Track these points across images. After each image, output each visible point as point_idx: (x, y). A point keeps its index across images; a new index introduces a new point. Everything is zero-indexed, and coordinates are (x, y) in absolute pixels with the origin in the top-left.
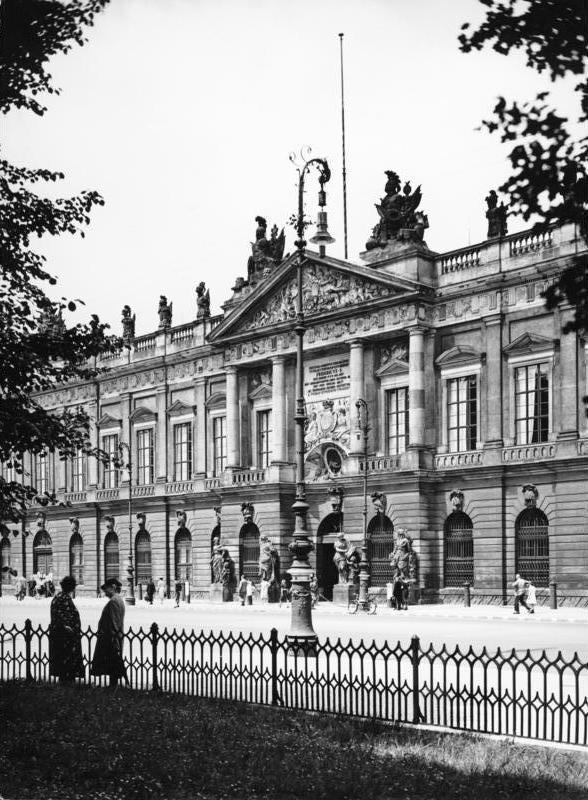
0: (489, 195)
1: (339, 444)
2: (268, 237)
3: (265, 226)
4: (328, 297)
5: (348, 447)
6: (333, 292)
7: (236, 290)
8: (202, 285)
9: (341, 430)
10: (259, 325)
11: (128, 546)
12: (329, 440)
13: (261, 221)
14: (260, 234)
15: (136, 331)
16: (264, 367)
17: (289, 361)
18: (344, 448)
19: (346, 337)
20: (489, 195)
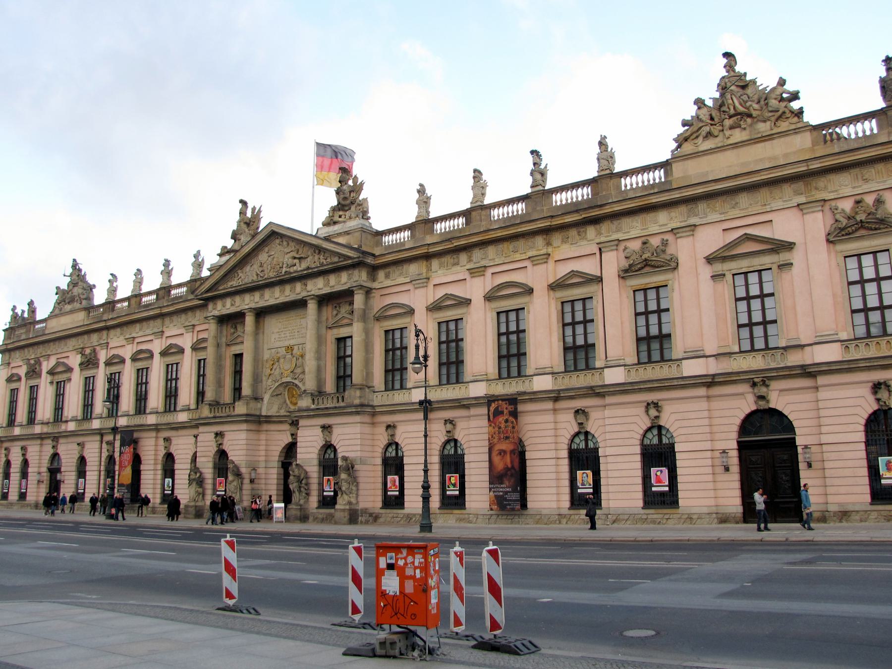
0: (419, 187)
1: (296, 382)
2: (249, 214)
3: (247, 207)
4: (291, 261)
5: (304, 384)
6: (295, 258)
7: (220, 255)
8: (199, 252)
9: (299, 370)
10: (234, 283)
11: (96, 468)
12: (289, 379)
13: (243, 203)
14: (242, 213)
15: (143, 287)
16: (237, 318)
17: (261, 313)
18: (300, 385)
19: (304, 294)
20: (419, 187)
